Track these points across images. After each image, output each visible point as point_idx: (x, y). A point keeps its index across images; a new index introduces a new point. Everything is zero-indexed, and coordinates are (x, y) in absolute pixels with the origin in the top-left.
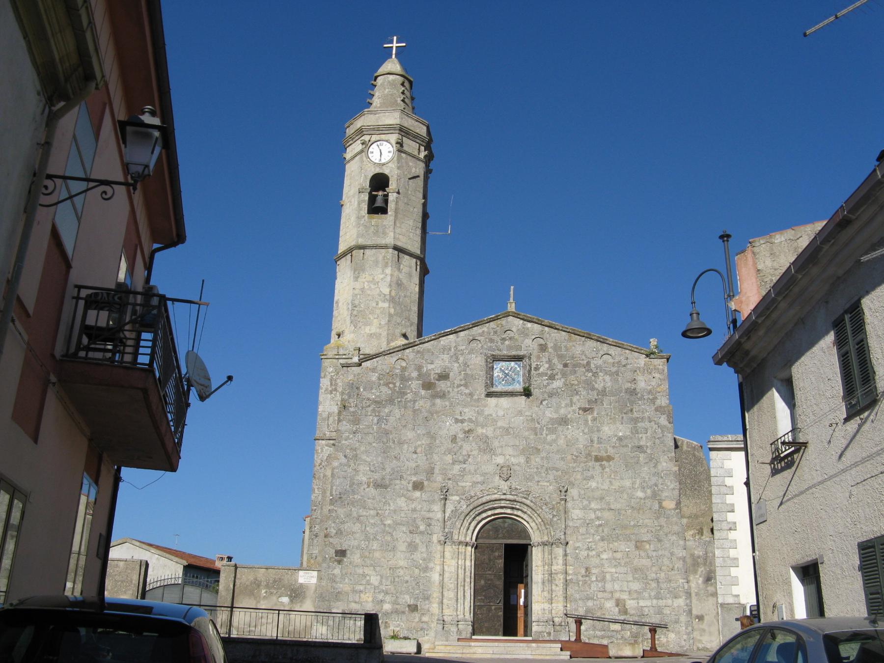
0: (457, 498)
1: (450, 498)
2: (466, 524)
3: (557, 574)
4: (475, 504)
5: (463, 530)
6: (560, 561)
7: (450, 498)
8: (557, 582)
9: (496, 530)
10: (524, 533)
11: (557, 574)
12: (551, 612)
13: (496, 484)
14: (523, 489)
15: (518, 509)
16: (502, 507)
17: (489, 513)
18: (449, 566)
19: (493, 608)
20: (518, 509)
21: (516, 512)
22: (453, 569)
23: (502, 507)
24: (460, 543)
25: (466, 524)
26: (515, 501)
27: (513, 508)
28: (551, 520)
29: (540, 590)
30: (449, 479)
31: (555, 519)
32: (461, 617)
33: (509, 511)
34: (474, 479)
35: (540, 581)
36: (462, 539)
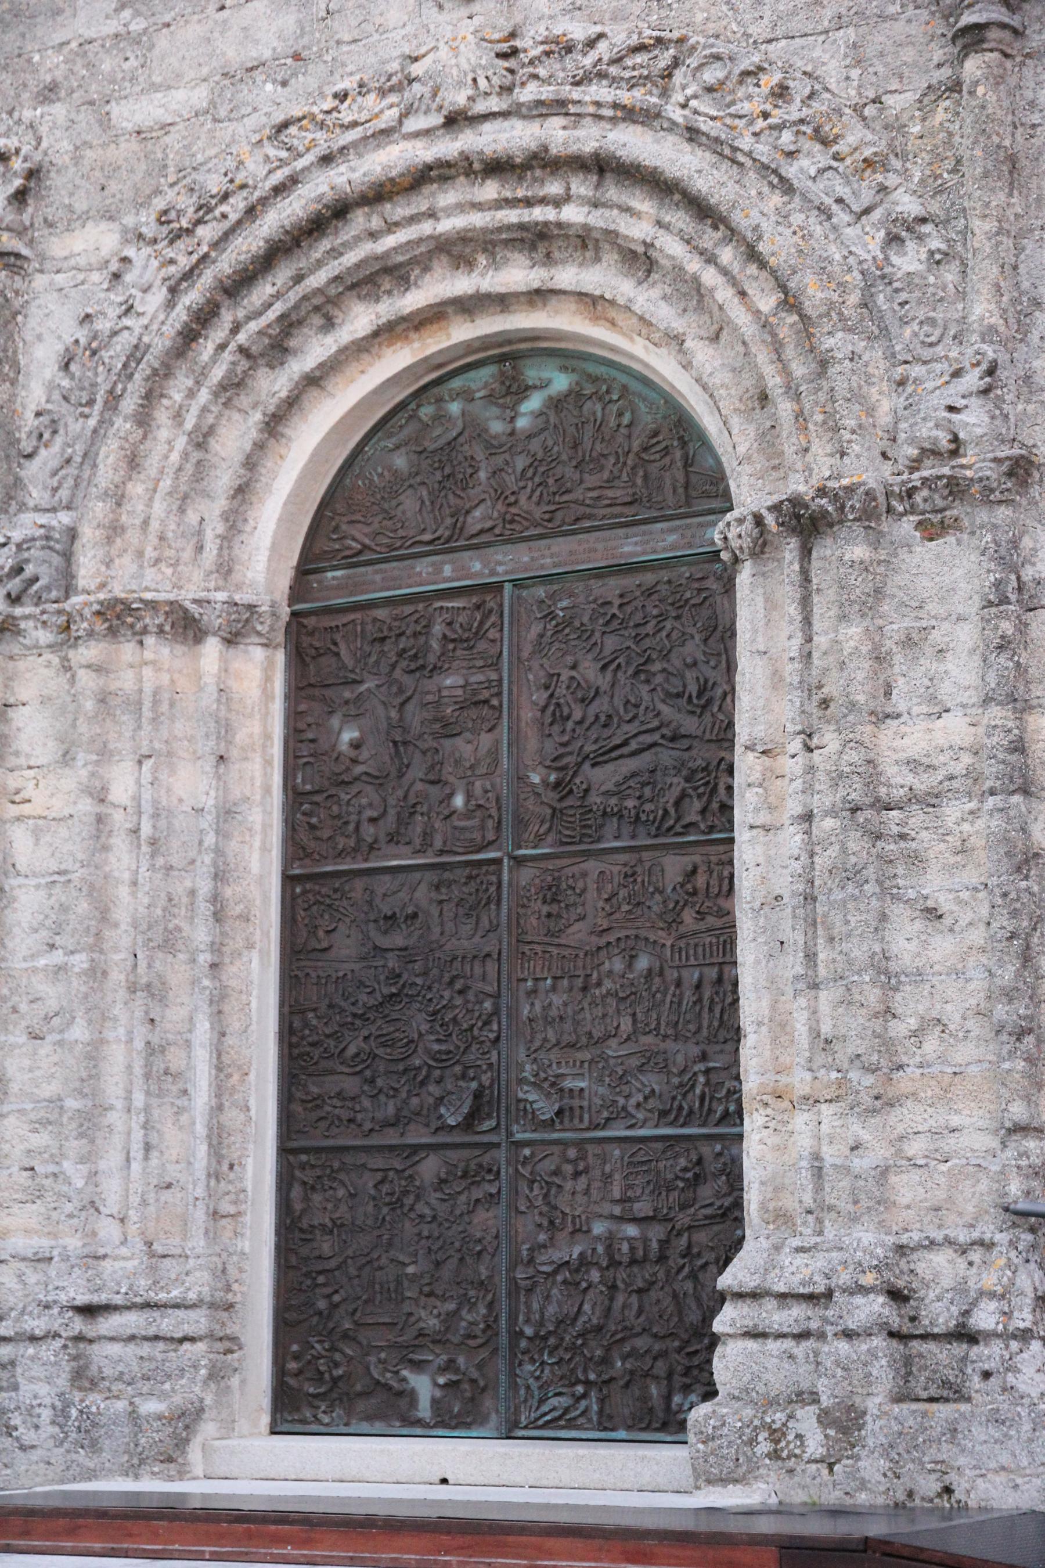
0: (99, 240)
1: (57, 246)
2: (168, 444)
3: (930, 801)
4: (226, 264)
5: (149, 502)
6: (962, 672)
7: (57, 246)
8: (935, 885)
9: (447, 467)
10: (674, 463)
11: (930, 801)
12: (875, 1193)
13: (385, 55)
14: (620, 37)
15: (586, 243)
16: (458, 250)
17: (360, 319)
18: (42, 825)
19: (430, 1168)
20: (586, 243)
21: (568, 276)
22: (69, 846)
23: (458, 250)
24: (119, 617)
25: (168, 444)
26: (542, 162)
27: (538, 240)
28: (875, 278)
29: (793, 964)
30: (49, 93)
31: (909, 260)
32: (122, 1272)
33: (517, 274)
34: (233, 52)
35: (784, 883)
36: (128, 579)
